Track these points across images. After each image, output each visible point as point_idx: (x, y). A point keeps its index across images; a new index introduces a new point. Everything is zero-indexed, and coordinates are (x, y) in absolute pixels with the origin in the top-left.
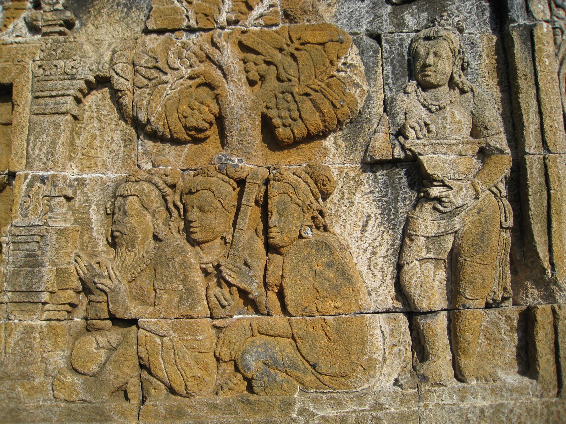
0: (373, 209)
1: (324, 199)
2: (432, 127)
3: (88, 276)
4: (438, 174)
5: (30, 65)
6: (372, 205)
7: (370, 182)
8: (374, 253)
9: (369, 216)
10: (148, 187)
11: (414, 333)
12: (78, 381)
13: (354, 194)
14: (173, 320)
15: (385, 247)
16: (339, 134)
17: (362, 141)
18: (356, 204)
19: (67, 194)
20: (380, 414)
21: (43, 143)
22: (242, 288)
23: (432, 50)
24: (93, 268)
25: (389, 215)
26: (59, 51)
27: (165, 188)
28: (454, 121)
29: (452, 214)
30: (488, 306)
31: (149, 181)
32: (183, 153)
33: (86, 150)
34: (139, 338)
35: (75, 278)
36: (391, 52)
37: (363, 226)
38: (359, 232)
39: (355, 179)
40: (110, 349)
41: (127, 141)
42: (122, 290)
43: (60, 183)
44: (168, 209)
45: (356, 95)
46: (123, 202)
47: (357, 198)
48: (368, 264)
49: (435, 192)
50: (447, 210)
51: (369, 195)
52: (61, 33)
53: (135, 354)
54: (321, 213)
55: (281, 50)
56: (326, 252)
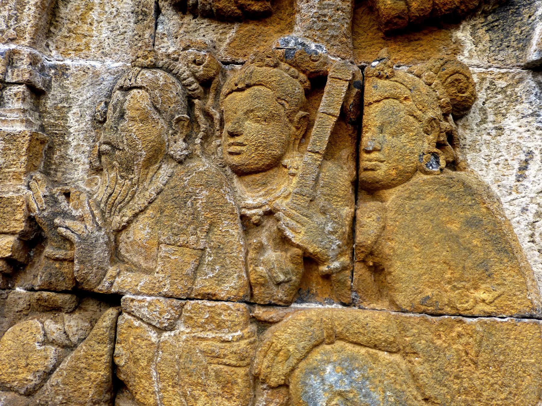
1: (456, 119)
3: (45, 213)
6: (536, 136)
7: (533, 98)
9: (530, 153)
10: (165, 78)
13: (504, 115)
14: (183, 302)
17: (518, 32)
18: (507, 132)
19: (32, 80)
22: (311, 250)
24: (56, 201)
27: (193, 83)
31: (169, 71)
32: (228, 36)
33: (74, 25)
34: (119, 329)
37: (520, 169)
38: (514, 178)
39: (505, 92)
40: (64, 347)
42: (101, 241)
46: (121, 98)
48: (530, 232)
51: (530, 119)
53: (106, 358)
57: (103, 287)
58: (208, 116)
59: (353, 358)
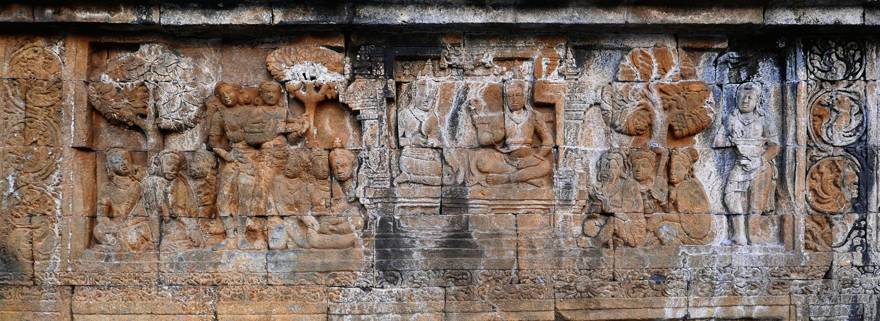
0: (714, 169)
2: (744, 132)
4: (746, 154)
5: (564, 95)
8: (713, 188)
11: (730, 224)
12: (588, 239)
15: (718, 186)
16: (700, 134)
20: (716, 256)
21: (571, 134)
23: (748, 95)
25: (720, 172)
26: (577, 89)
28: (755, 130)
29: (750, 172)
30: (763, 214)
35: (587, 195)
36: (727, 94)
41: (607, 134)
43: (579, 152)
44: (625, 165)
45: (711, 117)
47: (707, 164)
49: (743, 162)
50: (748, 170)
52: (576, 80)
54: (692, 169)
55: (679, 94)
56: (696, 186)
57: (610, 211)
58: (628, 164)
59: (668, 224)
